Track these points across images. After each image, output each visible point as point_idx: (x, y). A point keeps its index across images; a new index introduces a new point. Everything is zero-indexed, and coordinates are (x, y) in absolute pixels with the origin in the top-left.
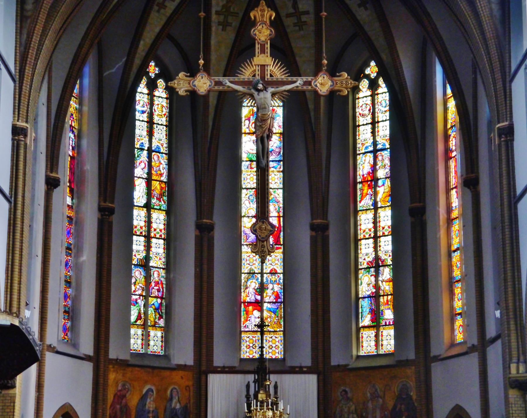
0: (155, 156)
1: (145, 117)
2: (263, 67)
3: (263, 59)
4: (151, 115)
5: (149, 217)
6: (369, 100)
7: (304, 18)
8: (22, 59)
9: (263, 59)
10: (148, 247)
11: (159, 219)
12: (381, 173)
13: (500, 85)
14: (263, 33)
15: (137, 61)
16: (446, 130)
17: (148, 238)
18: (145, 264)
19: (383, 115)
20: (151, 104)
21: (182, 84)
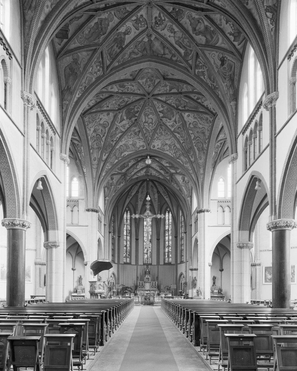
0: (128, 226)
1: (126, 218)
2: (148, 213)
3: (148, 211)
4: (127, 218)
5: (127, 237)
6: (168, 215)
7: (156, 199)
8: (105, 212)
9: (148, 211)
10: (127, 243)
11: (128, 238)
12: (170, 229)
13: (190, 217)
14: (148, 207)
15: (124, 208)
16: (182, 222)
17: (127, 241)
18: (126, 246)
19: (170, 218)
20: (127, 216)
21: (133, 216)
